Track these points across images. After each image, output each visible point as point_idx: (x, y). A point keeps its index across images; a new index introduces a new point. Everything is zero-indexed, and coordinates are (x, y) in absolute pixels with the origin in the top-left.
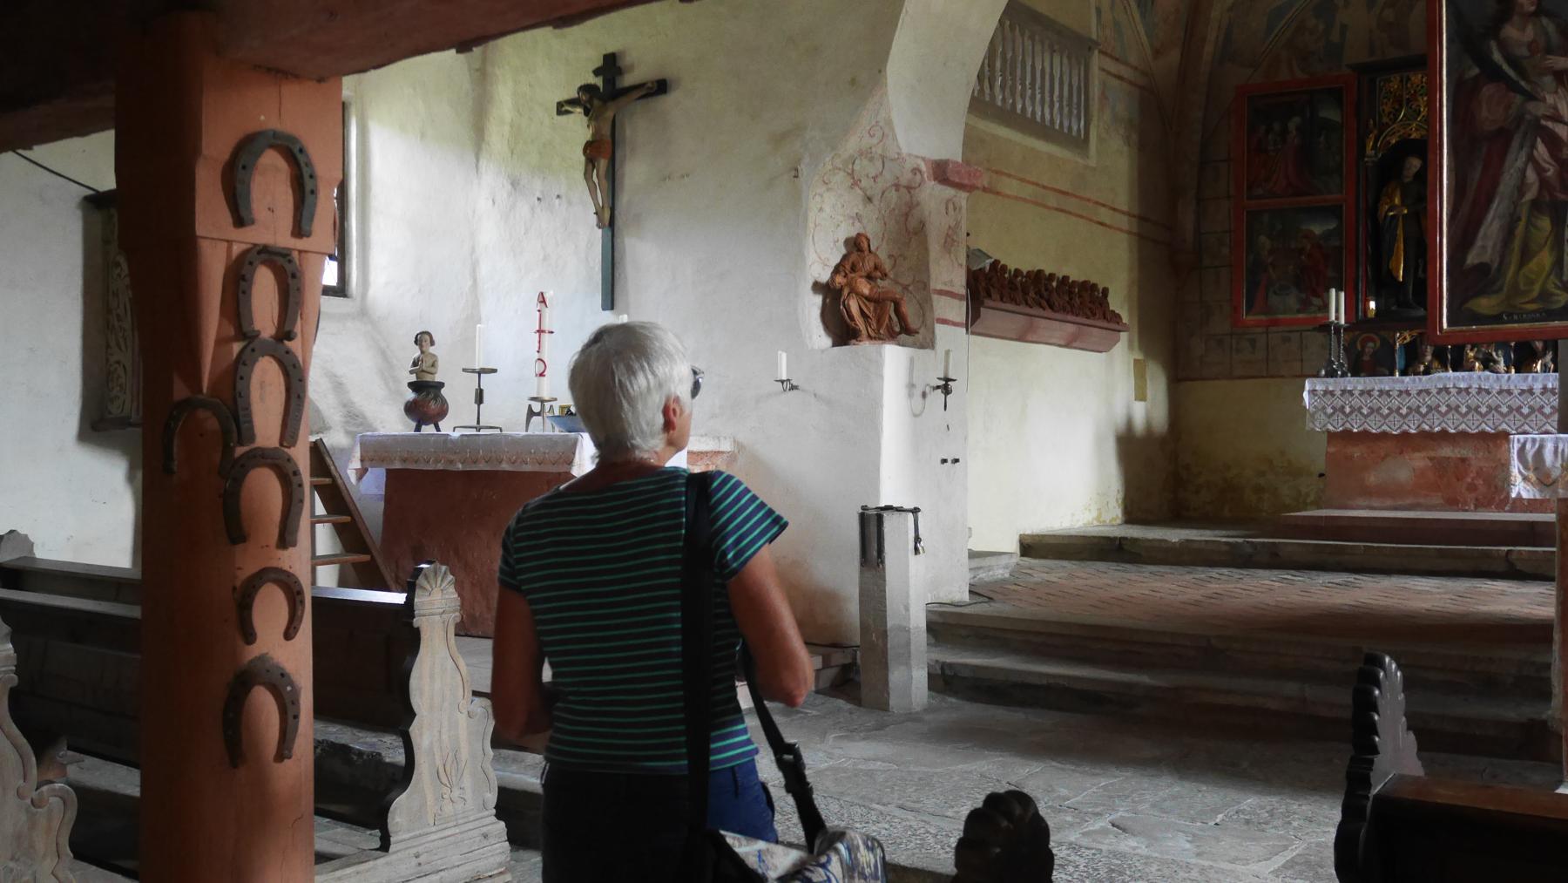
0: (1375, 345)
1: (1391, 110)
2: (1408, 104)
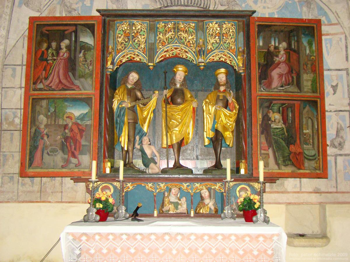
1: (123, 41)
2: (133, 39)
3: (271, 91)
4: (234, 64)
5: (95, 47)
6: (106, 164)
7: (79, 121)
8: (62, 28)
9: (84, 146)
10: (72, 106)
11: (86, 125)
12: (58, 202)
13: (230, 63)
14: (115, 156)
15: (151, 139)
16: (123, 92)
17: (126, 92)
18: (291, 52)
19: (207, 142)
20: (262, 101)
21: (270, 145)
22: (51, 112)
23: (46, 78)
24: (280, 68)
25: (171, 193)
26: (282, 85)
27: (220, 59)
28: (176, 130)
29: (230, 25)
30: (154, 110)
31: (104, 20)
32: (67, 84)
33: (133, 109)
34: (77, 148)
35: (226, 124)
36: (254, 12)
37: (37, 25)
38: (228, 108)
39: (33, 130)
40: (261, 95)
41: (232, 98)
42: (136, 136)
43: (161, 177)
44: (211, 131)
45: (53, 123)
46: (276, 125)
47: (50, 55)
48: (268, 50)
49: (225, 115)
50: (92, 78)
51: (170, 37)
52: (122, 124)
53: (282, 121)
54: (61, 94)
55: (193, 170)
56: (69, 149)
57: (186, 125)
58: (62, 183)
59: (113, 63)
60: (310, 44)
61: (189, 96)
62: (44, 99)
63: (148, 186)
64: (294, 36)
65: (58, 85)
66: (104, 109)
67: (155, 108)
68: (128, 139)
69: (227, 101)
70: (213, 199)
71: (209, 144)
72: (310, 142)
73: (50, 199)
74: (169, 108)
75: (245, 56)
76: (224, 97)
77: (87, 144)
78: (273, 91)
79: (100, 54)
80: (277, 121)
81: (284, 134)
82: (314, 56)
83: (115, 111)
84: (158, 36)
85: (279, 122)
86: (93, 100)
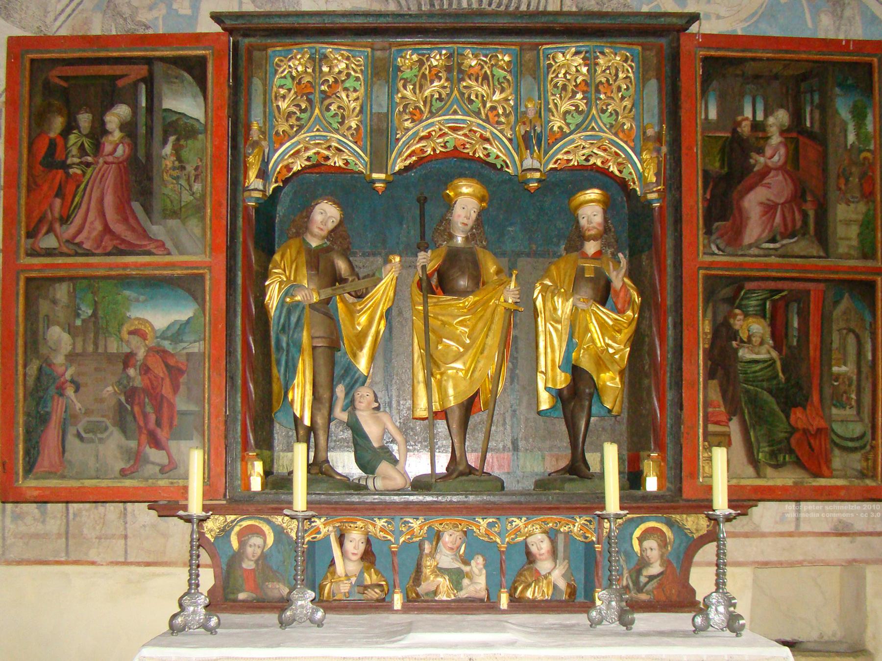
0: (265, 542)
1: (293, 109)
2: (323, 100)
3: (740, 253)
4: (631, 173)
5: (209, 127)
6: (249, 466)
7: (167, 345)
8: (106, 70)
9: (184, 413)
10: (146, 300)
11: (188, 354)
12: (117, 563)
13: (617, 173)
14: (276, 442)
15: (379, 395)
16: (296, 259)
17: (303, 258)
18: (802, 139)
19: (545, 401)
20: (713, 285)
21: (733, 409)
22: (82, 317)
23: (65, 220)
24: (768, 186)
25: (441, 543)
26: (771, 235)
27: (587, 160)
28: (458, 370)
29: (618, 58)
30: (389, 311)
31: (236, 45)
32: (129, 236)
33: (325, 308)
34: (165, 421)
35: (602, 351)
36: (694, 18)
37: (32, 61)
38: (610, 301)
39: (33, 369)
40: (710, 266)
41: (625, 276)
42: (337, 384)
43: (412, 503)
44: (558, 370)
45: (90, 348)
46: (752, 352)
47: (75, 151)
48: (734, 131)
49: (602, 325)
50: (203, 218)
51: (436, 96)
52: (293, 350)
53: (771, 342)
54: (111, 267)
55: (503, 477)
56: (142, 424)
57: (486, 353)
58: (125, 515)
59: (263, 174)
60: (859, 115)
61: (493, 269)
62: (61, 279)
63: (374, 526)
64: (812, 92)
65: (99, 242)
66: (239, 310)
67: (390, 304)
68: (314, 394)
69: (608, 283)
70: (564, 559)
71: (553, 408)
72: (849, 399)
73: (93, 555)
74: (435, 304)
75: (664, 149)
76: (599, 272)
77: (193, 407)
78: (747, 252)
79: (226, 145)
80: (756, 340)
81: (776, 377)
82: (869, 151)
83: (272, 314)
84: (398, 91)
85: (762, 343)
86: (208, 283)
